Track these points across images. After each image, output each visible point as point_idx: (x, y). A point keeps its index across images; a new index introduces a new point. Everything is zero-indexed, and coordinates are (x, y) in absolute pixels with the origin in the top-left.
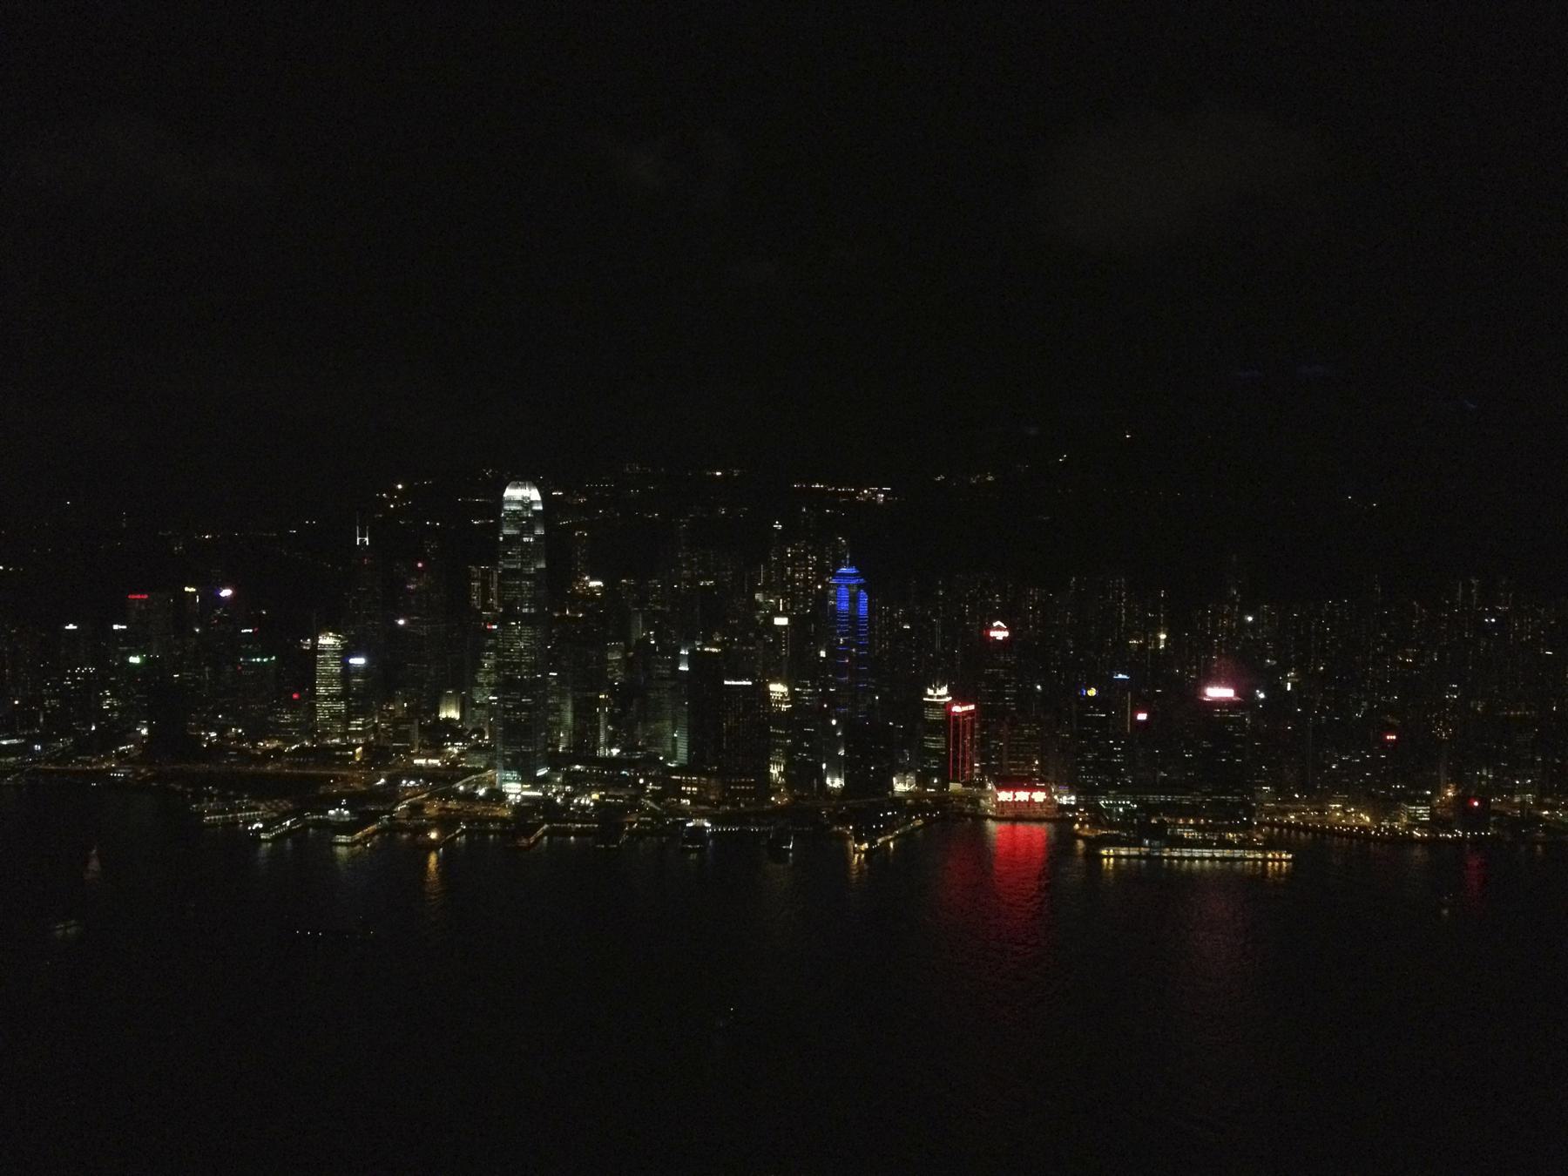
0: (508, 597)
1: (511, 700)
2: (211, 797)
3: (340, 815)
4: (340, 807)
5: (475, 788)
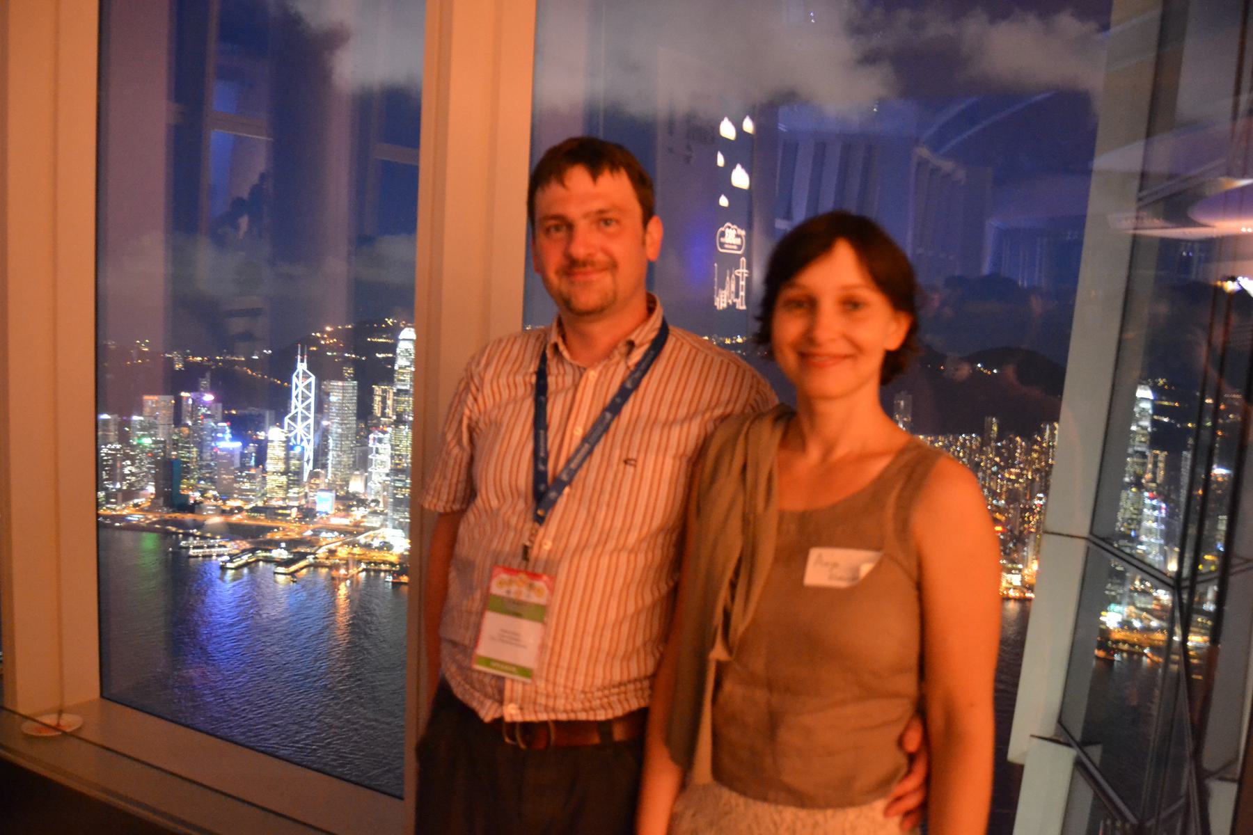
0: (400, 409)
1: (398, 480)
2: (194, 536)
3: (280, 554)
4: (281, 548)
5: (372, 540)
